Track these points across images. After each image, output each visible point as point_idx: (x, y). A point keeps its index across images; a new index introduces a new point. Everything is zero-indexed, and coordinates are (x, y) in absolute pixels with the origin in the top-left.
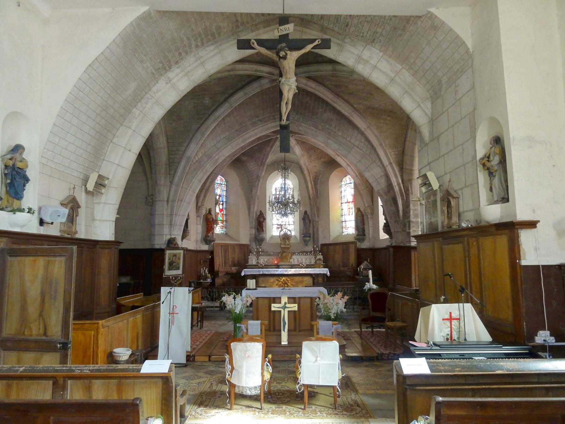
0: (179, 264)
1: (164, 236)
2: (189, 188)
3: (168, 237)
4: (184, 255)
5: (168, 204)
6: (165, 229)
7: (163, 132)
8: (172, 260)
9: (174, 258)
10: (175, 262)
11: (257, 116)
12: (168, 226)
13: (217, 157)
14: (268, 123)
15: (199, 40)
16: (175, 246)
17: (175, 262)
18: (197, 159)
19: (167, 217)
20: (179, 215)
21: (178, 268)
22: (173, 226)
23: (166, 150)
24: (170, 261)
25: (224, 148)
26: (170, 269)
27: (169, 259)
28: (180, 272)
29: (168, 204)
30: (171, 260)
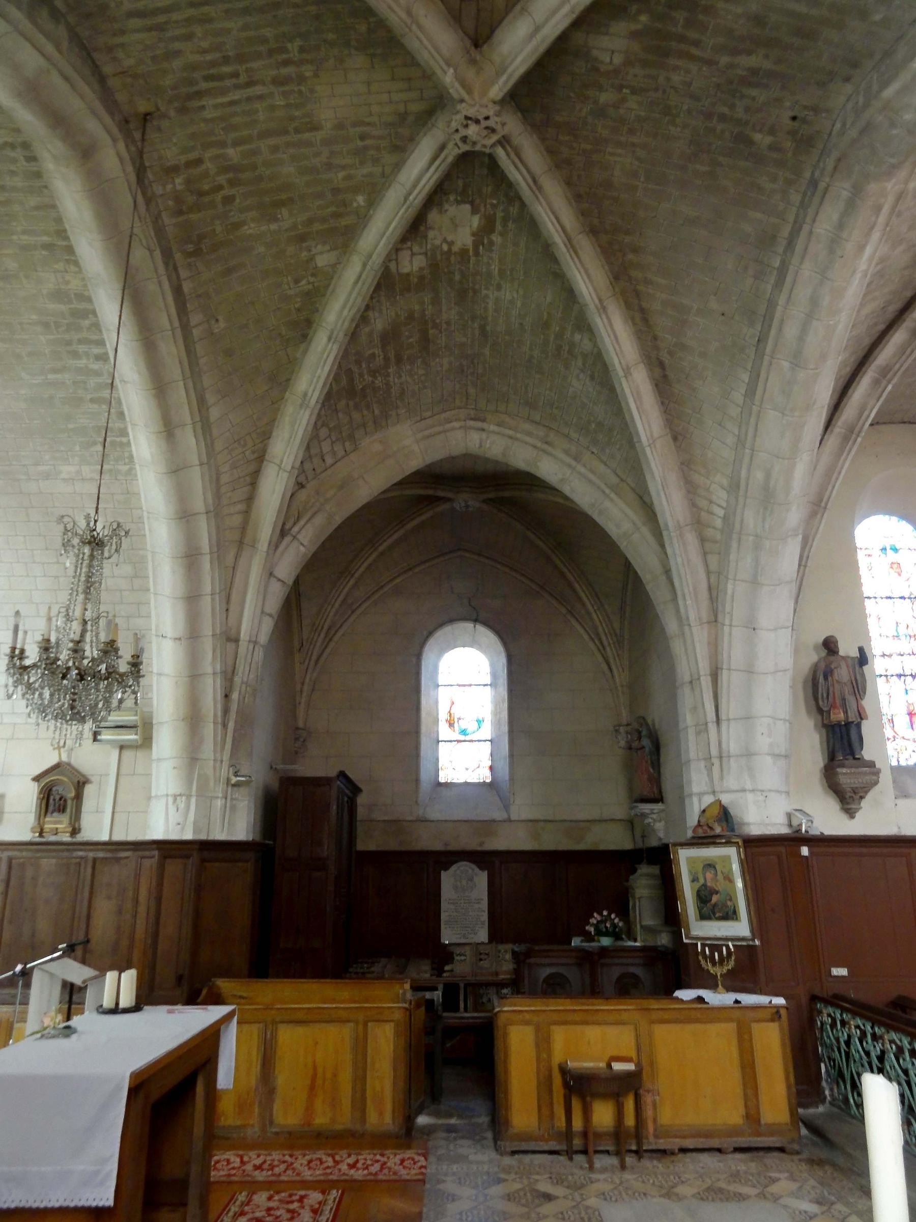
0: (731, 897)
1: (695, 800)
2: (727, 622)
3: (708, 800)
4: (750, 869)
5: (692, 689)
6: (694, 776)
7: (607, 491)
8: (705, 885)
9: (709, 875)
10: (717, 892)
11: (767, 240)
12: (702, 764)
13: (759, 475)
14: (806, 228)
15: (82, 348)
16: (711, 833)
17: (717, 892)
18: (721, 512)
19: (698, 733)
20: (729, 720)
21: (730, 915)
22: (716, 761)
23: (645, 531)
24: (697, 886)
25: (756, 430)
26: (703, 917)
27: (694, 880)
28: (741, 928)
29: (692, 689)
30: (702, 881)
